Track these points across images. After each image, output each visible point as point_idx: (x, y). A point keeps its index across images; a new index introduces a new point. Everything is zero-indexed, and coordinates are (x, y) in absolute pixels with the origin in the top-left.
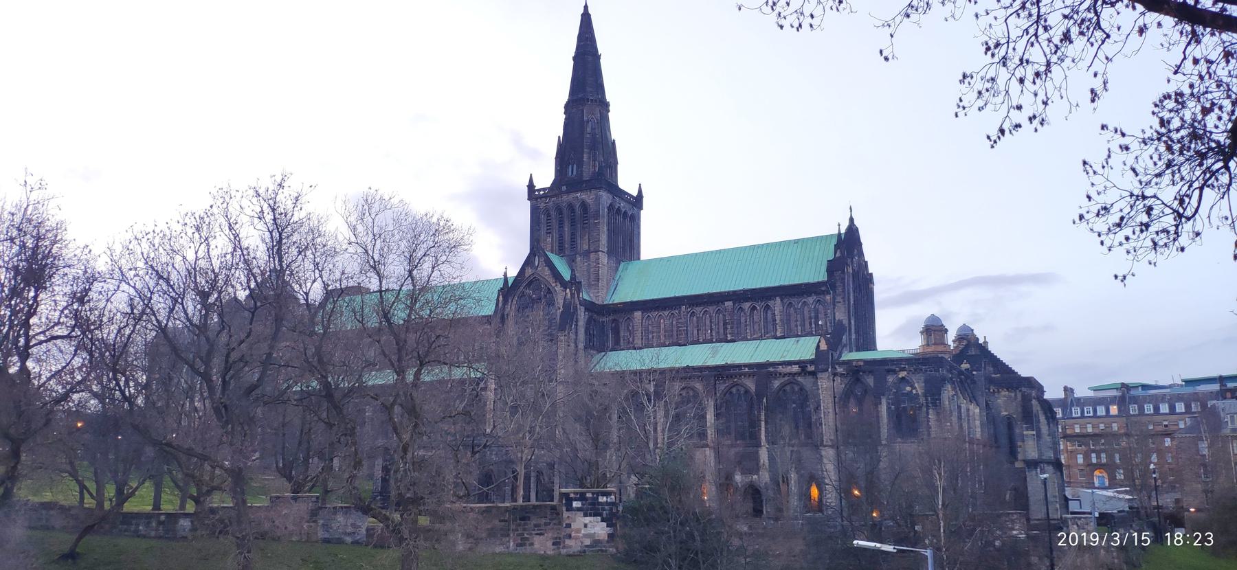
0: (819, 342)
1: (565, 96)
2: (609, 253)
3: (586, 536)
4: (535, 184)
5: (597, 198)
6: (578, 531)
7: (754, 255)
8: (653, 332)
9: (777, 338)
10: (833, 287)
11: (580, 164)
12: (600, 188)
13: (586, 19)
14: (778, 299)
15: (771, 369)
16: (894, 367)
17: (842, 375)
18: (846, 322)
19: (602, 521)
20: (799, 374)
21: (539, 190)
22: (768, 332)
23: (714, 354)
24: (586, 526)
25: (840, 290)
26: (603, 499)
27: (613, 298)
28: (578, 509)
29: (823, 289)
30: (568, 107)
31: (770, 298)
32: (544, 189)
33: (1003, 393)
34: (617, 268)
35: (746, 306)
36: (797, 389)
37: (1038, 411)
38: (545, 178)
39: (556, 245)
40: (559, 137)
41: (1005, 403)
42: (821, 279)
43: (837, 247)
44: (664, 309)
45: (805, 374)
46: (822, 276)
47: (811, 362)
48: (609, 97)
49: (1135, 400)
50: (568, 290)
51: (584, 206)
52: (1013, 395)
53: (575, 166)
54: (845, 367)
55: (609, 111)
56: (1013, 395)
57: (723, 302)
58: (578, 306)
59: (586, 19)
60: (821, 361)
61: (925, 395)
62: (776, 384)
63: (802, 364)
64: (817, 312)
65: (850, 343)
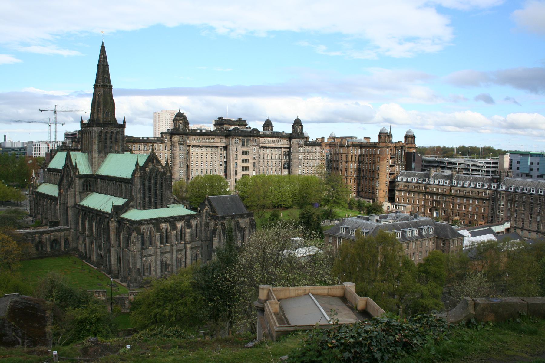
2: (100, 152)
29: (131, 182)
31: (121, 182)
34: (105, 157)
35: (118, 183)
37: (220, 230)
46: (131, 178)
57: (113, 181)
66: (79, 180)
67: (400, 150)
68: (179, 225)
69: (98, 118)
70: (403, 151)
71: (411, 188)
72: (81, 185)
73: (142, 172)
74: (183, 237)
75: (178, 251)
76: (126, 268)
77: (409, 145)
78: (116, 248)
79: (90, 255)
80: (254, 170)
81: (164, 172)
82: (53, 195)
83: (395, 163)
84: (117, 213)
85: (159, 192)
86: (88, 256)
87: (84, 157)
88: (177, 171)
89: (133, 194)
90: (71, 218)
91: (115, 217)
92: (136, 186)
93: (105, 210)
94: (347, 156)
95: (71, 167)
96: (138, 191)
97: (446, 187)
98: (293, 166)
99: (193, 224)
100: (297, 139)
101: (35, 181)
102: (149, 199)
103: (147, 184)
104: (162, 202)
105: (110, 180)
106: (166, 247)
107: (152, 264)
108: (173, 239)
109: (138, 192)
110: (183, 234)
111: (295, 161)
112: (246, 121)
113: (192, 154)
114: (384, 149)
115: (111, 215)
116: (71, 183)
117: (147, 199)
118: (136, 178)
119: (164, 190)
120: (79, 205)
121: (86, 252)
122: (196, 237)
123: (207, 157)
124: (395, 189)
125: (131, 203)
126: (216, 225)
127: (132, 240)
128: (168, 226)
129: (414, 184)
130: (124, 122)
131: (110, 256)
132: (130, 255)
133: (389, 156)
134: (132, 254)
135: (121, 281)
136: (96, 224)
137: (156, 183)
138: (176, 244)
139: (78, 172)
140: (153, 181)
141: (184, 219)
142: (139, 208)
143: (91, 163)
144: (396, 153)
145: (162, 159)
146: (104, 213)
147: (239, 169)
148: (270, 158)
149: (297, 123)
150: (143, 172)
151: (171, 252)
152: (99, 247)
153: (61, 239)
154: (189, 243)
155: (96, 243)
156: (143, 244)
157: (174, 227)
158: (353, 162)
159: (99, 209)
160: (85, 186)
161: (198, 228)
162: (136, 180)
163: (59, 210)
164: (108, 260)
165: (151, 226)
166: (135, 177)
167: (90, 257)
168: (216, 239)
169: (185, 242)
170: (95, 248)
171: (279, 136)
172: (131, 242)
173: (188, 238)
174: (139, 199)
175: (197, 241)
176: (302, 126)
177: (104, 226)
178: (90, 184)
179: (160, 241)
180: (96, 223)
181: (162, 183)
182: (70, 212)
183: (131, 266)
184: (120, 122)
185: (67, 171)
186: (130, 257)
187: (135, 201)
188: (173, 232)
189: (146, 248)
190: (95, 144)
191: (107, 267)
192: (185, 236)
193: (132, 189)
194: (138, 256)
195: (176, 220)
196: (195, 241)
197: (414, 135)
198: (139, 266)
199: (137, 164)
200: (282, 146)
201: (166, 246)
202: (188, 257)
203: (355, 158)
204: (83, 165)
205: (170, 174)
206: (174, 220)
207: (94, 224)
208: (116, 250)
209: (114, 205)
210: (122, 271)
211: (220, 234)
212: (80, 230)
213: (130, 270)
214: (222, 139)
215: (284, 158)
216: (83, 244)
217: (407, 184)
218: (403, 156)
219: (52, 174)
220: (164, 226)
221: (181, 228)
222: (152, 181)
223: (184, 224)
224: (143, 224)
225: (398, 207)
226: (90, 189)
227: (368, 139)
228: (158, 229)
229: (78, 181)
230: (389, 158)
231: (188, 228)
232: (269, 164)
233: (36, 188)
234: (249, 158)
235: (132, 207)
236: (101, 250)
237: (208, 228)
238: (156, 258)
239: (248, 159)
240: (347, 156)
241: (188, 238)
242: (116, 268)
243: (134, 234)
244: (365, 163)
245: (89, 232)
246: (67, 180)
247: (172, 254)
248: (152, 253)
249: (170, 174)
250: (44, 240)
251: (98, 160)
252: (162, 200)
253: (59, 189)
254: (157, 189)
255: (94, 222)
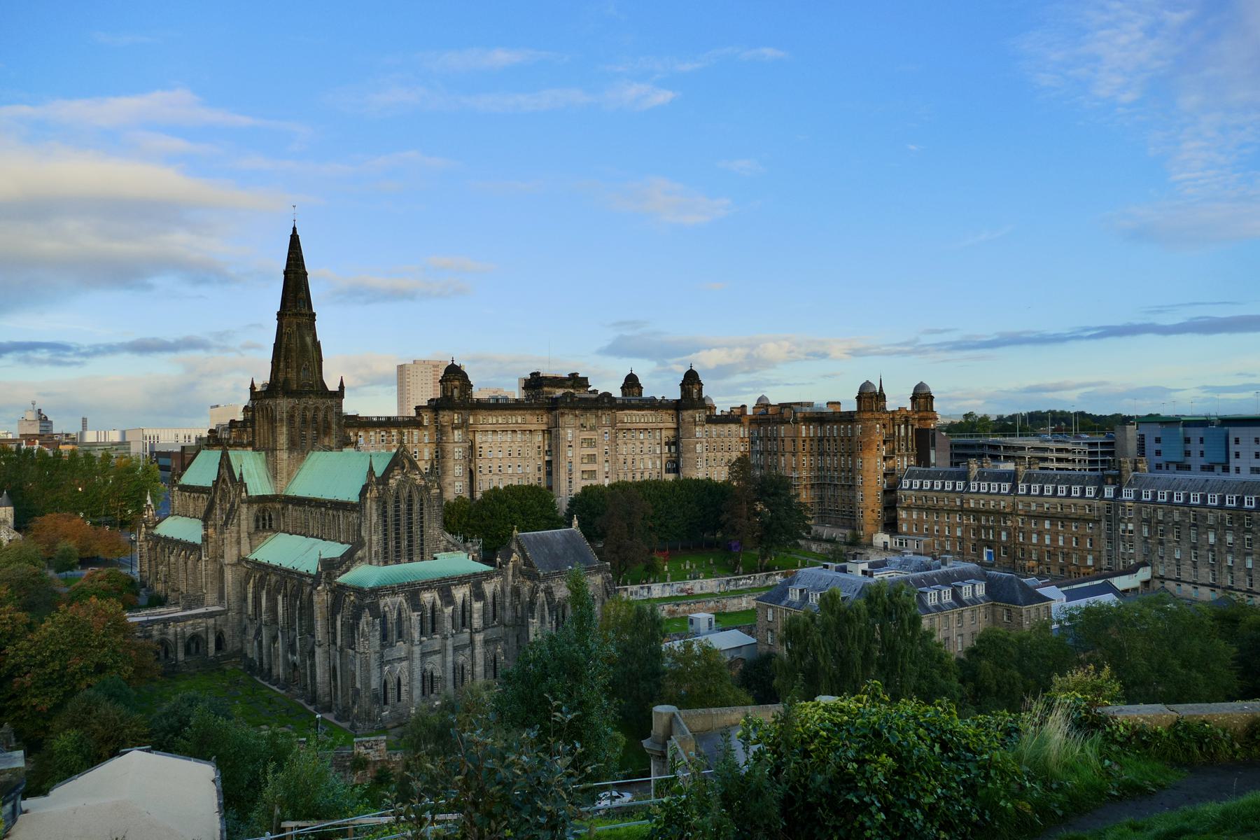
13: (295, 241)
34: (303, 459)
35: (331, 512)
59: (295, 241)
66: (248, 508)
67: (903, 426)
68: (460, 593)
69: (286, 381)
70: (910, 427)
71: (930, 503)
72: (252, 520)
73: (381, 487)
74: (468, 619)
75: (456, 649)
76: (348, 690)
77: (921, 414)
78: (327, 648)
79: (270, 665)
80: (607, 477)
81: (426, 487)
82: (191, 540)
83: (894, 453)
84: (328, 575)
85: (416, 528)
86: (266, 666)
87: (259, 461)
88: (450, 484)
89: (363, 533)
90: (230, 589)
91: (325, 583)
92: (368, 515)
93: (302, 569)
94: (794, 441)
95: (231, 483)
96: (373, 527)
97: (1005, 497)
98: (686, 466)
99: (487, 591)
100: (690, 412)
101: (151, 512)
102: (396, 543)
103: (391, 511)
104: (422, 549)
106: (431, 641)
107: (402, 680)
108: (446, 625)
109: (373, 530)
110: (467, 614)
111: (688, 455)
112: (586, 379)
113: (481, 448)
114: (869, 423)
115: (316, 579)
116: (231, 514)
117: (392, 544)
118: (369, 501)
119: (426, 524)
120: (247, 561)
121: (261, 659)
122: (495, 619)
123: (510, 455)
124: (897, 505)
125: (359, 552)
126: (534, 592)
127: (361, 628)
128: (437, 597)
129: (937, 494)
130: (342, 387)
131: (313, 665)
132: (358, 662)
133: (881, 438)
134: (361, 658)
135: (336, 718)
136: (283, 599)
137: (410, 509)
138: (453, 635)
139: (246, 491)
140: (403, 506)
141: (469, 582)
142: (375, 562)
143: (274, 473)
144: (894, 432)
145: (419, 460)
146: (301, 575)
147: (577, 475)
148: (638, 450)
149: (691, 379)
150: (383, 489)
151: (442, 651)
152: (291, 648)
153: (207, 632)
154: (479, 632)
155: (282, 638)
156: (384, 637)
157: (448, 599)
158: (808, 454)
159: (290, 567)
160: (261, 519)
161: (498, 600)
162: (368, 505)
163: (204, 573)
164: (308, 673)
165: (400, 599)
166: (366, 499)
167: (270, 669)
168: (535, 621)
169: (471, 630)
170: (280, 650)
171: (654, 405)
172: (358, 634)
173: (477, 622)
174: (374, 542)
175: (495, 626)
176: (700, 384)
177: (301, 603)
178: (270, 516)
179: (419, 630)
180: (285, 596)
181: (422, 509)
182: (229, 575)
183: (358, 685)
184: (332, 386)
185: (223, 490)
186: (358, 667)
187: (366, 548)
188: (446, 610)
189: (391, 645)
190: (282, 434)
191: (306, 689)
192: (471, 617)
193: (360, 523)
194: (374, 663)
195: (453, 585)
196: (493, 627)
197: (930, 393)
198: (375, 683)
199: (371, 470)
200: (661, 425)
201: (432, 638)
202: (478, 661)
203: (812, 445)
204: (256, 476)
205: (438, 491)
206: (450, 585)
207: (280, 598)
208: (326, 652)
209: (322, 557)
210: (340, 696)
211: (543, 610)
212: (250, 613)
213: (357, 692)
214: (540, 417)
215: (667, 451)
216: (256, 643)
217: (922, 493)
218: (910, 438)
219: (189, 496)
220: (427, 597)
221: (464, 601)
222: (402, 506)
223: (468, 593)
224: (384, 595)
225: (906, 543)
226: (270, 526)
227: (837, 406)
228: (415, 603)
229: (246, 509)
230: (882, 443)
231: (476, 601)
232: (637, 462)
233: (154, 527)
234: (596, 453)
235: (361, 559)
236: (294, 653)
237: (519, 598)
238: (410, 665)
239: (595, 455)
240: (794, 441)
241: (477, 622)
242: (327, 689)
243: (366, 617)
244: (832, 454)
245: (269, 616)
246: (222, 509)
247: (444, 657)
248: (403, 654)
249: (438, 491)
250: (171, 637)
251: (288, 466)
252: (422, 544)
253: (206, 527)
254: (412, 523)
255: (280, 593)
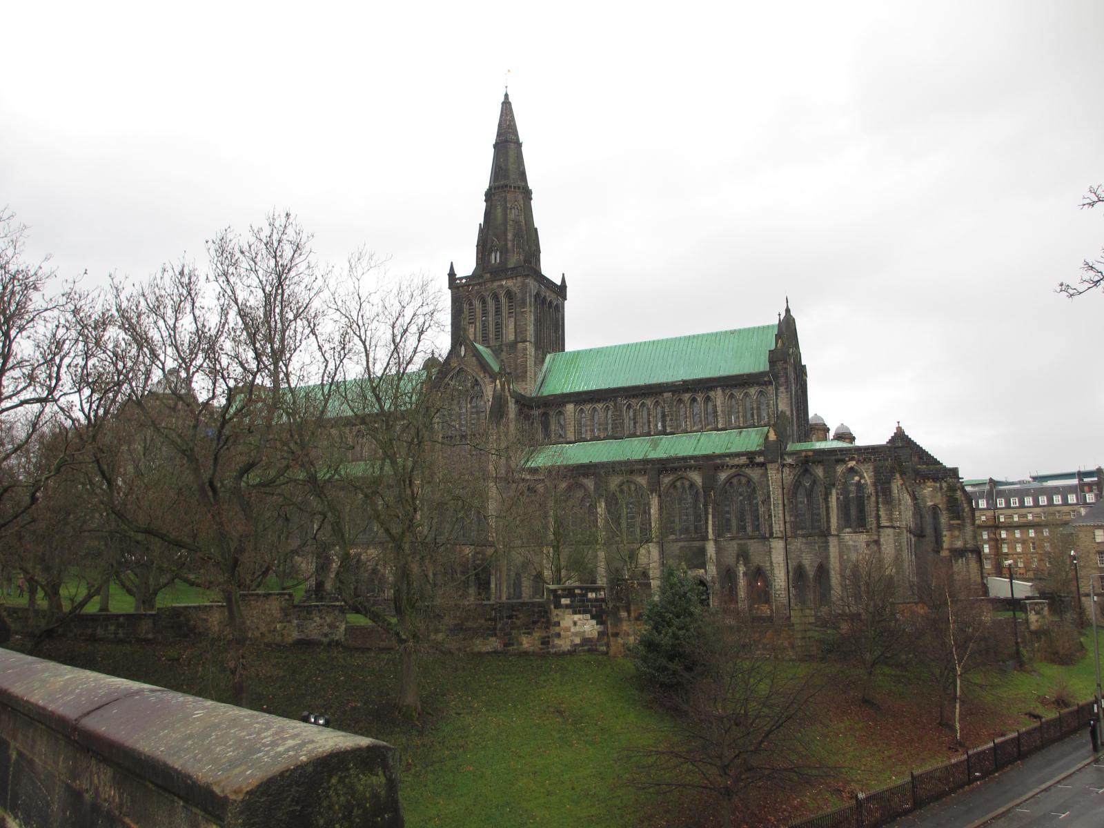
0: (768, 432)
1: (485, 184)
3: (576, 634)
4: (456, 272)
5: (524, 286)
6: (568, 629)
7: (690, 346)
8: (586, 426)
9: (718, 430)
10: (776, 377)
11: (504, 252)
12: (527, 276)
13: (506, 106)
14: (719, 391)
15: (718, 461)
16: (843, 457)
17: (791, 465)
18: (788, 413)
19: (593, 618)
20: (748, 465)
21: (461, 279)
22: (710, 423)
23: (655, 446)
24: (575, 624)
25: (782, 380)
26: (591, 595)
27: (542, 390)
28: (567, 606)
29: (766, 379)
30: (489, 196)
31: (712, 388)
32: (466, 278)
33: (929, 484)
35: (686, 396)
36: (744, 480)
38: (467, 266)
39: (479, 334)
40: (480, 225)
41: (930, 494)
42: (762, 369)
43: (778, 337)
44: (599, 401)
45: (753, 465)
46: (767, 369)
47: (760, 453)
48: (532, 184)
49: (1001, 494)
50: (498, 381)
51: (510, 295)
52: (938, 485)
53: (498, 254)
54: (794, 457)
55: (531, 199)
56: (938, 485)
57: (661, 393)
58: (509, 398)
59: (506, 106)
60: (772, 453)
61: (875, 484)
62: (723, 476)
63: (750, 455)
64: (759, 404)
65: (793, 434)
97: (985, 512)
105: (635, 396)
